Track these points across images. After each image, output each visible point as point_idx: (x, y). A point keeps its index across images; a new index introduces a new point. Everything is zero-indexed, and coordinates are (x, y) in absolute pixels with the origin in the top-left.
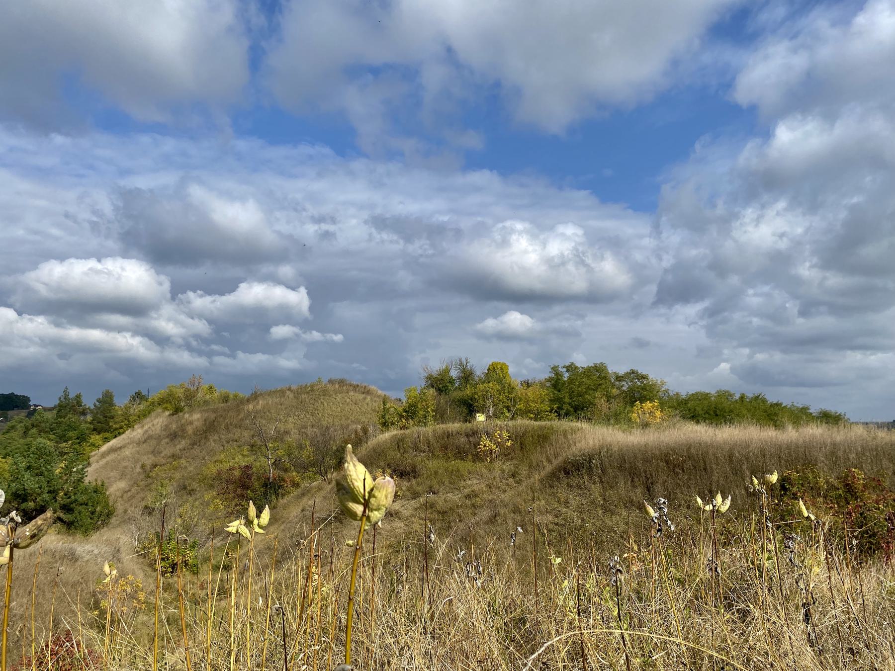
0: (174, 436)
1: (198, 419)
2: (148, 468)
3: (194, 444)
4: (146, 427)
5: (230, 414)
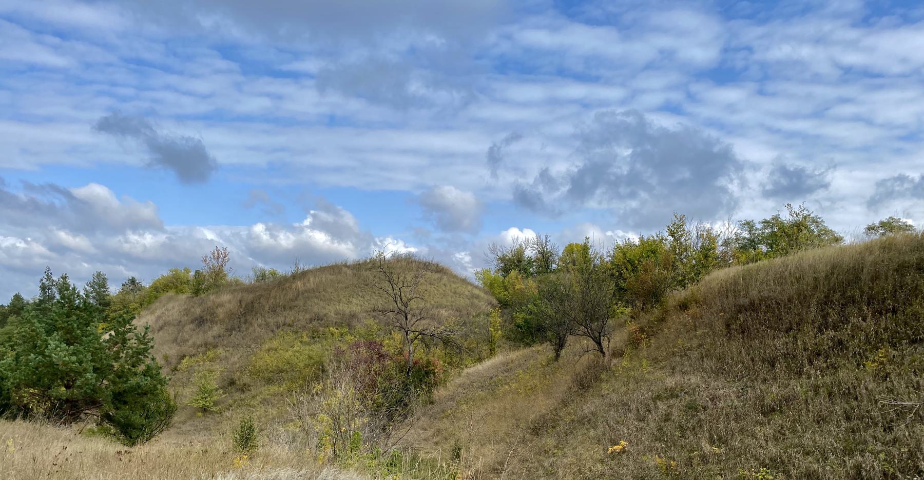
0: (200, 322)
1: (230, 302)
2: (174, 361)
3: (233, 329)
4: (158, 313)
5: (273, 293)
